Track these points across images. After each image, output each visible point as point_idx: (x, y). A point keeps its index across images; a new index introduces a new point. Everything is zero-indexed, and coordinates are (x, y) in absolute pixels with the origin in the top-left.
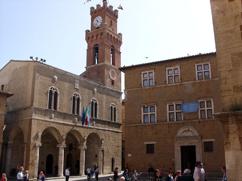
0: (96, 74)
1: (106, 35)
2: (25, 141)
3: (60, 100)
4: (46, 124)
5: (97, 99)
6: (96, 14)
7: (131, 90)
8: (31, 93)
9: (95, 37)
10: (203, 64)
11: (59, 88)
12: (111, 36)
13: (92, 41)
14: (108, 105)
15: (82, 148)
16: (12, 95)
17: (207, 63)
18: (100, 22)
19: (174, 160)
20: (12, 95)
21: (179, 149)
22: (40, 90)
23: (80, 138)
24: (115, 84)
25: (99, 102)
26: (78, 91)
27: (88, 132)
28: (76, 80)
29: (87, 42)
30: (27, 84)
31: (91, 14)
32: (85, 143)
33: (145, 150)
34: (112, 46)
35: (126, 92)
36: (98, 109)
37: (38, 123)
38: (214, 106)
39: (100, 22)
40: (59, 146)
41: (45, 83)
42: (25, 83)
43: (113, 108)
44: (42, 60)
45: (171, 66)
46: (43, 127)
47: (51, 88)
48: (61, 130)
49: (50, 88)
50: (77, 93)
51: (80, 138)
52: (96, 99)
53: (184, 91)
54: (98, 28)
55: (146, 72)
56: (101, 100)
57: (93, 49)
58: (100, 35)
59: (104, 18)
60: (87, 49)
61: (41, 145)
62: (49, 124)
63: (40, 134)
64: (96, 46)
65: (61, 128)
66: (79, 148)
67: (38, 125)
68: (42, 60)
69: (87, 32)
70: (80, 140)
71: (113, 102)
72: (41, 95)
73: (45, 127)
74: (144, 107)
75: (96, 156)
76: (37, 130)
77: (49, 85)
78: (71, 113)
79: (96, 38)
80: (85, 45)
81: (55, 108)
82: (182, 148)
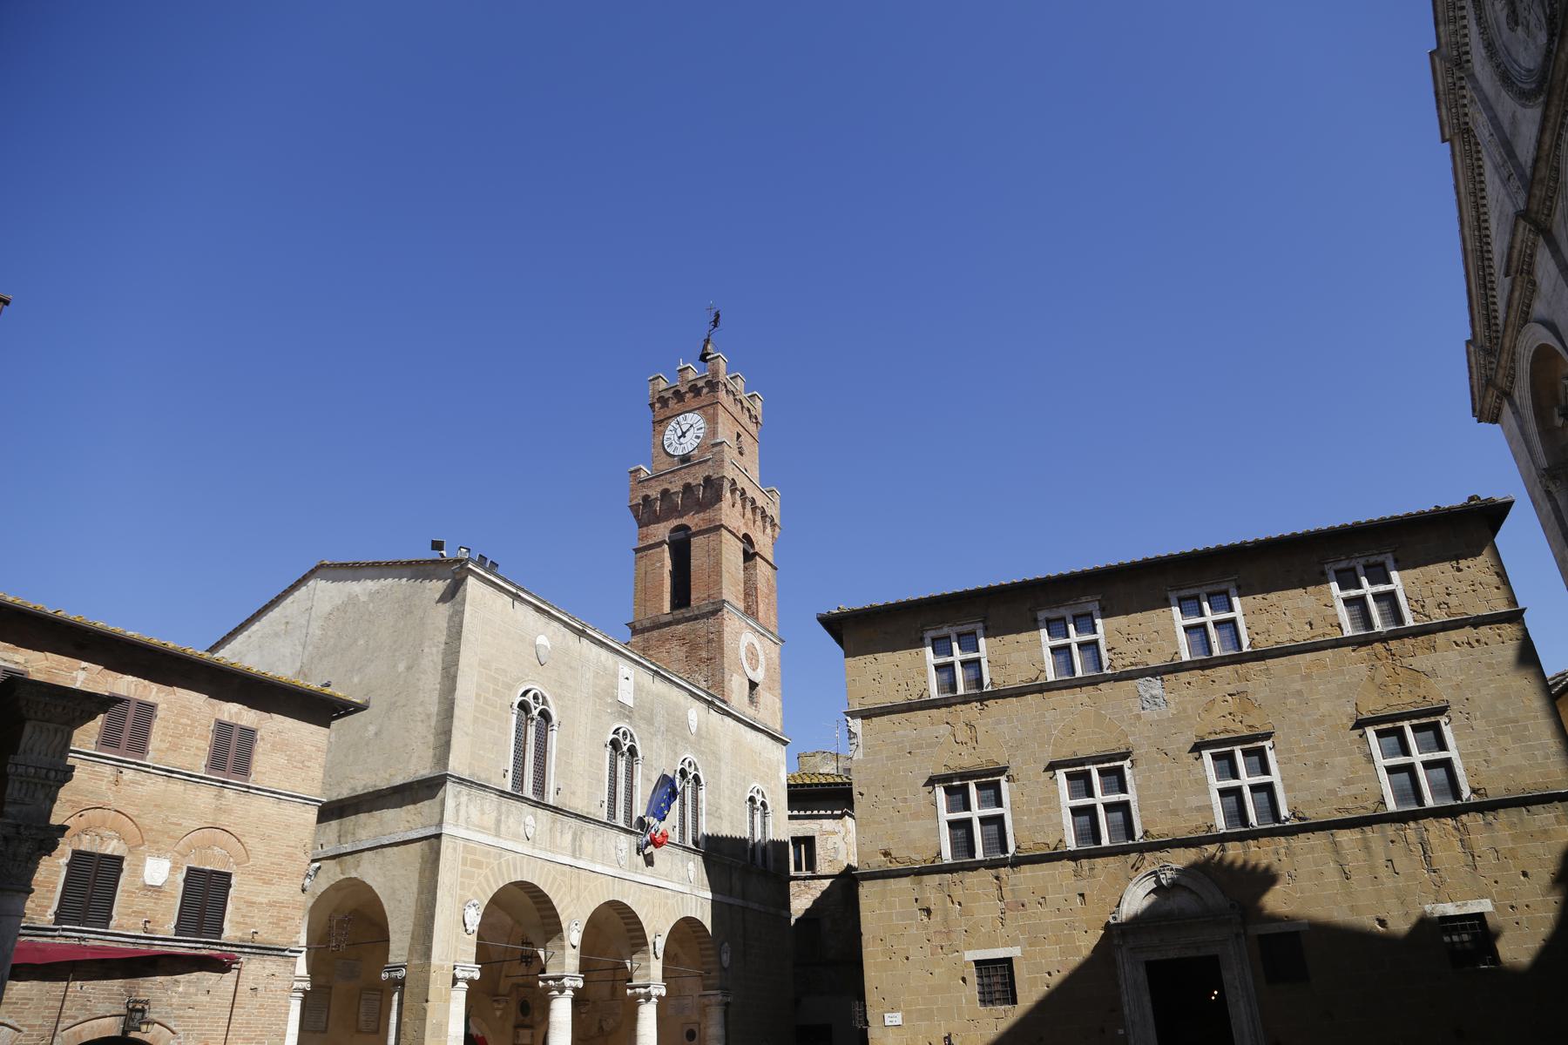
0: (682, 655)
2: (399, 949)
3: (560, 751)
10: (1202, 592)
11: (558, 697)
12: (743, 492)
14: (739, 791)
16: (359, 708)
17: (1223, 587)
19: (1121, 1032)
20: (359, 708)
21: (1142, 975)
22: (478, 696)
26: (629, 717)
30: (409, 668)
32: (656, 968)
33: (973, 989)
34: (746, 536)
36: (703, 806)
37: (464, 863)
38: (1281, 770)
42: (401, 667)
44: (483, 559)
45: (1059, 603)
47: (525, 693)
48: (561, 900)
50: (625, 726)
53: (1130, 711)
54: (685, 459)
55: (945, 630)
59: (712, 421)
61: (477, 976)
63: (474, 918)
64: (681, 535)
68: (483, 559)
73: (496, 882)
74: (948, 791)
75: (691, 1035)
78: (603, 815)
81: (540, 786)
82: (1152, 968)
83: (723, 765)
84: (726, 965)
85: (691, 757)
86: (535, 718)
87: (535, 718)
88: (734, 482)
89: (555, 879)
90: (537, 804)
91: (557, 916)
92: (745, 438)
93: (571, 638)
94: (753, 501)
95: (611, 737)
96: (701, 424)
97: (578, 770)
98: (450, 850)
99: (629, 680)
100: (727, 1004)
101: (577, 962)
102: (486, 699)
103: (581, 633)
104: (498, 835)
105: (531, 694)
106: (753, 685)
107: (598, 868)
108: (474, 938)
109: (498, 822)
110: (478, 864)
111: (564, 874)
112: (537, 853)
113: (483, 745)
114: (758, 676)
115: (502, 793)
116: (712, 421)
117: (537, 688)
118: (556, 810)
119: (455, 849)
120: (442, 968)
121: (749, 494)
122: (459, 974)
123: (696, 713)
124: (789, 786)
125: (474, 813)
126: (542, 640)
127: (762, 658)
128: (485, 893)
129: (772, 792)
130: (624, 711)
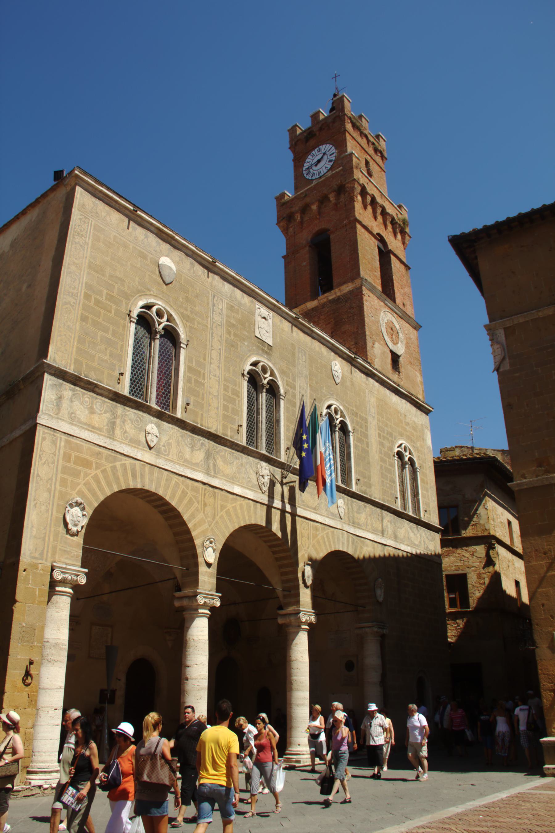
1: (358, 189)
3: (189, 369)
4: (114, 468)
5: (344, 406)
6: (312, 142)
7: (521, 320)
8: (43, 308)
9: (314, 207)
11: (184, 317)
12: (373, 199)
13: (302, 222)
14: (387, 444)
15: (292, 618)
18: (330, 161)
22: (87, 297)
23: (282, 574)
24: (402, 370)
25: (352, 422)
27: (318, 542)
28: (257, 306)
29: (285, 231)
31: (293, 147)
32: (306, 596)
35: (501, 334)
37: (67, 458)
39: (330, 161)
40: (185, 602)
41: (118, 274)
43: (406, 459)
46: (98, 482)
47: (148, 307)
48: (193, 516)
49: (141, 303)
50: (264, 361)
51: (282, 574)
52: (342, 408)
56: (361, 417)
57: (307, 248)
58: (332, 197)
60: (284, 253)
61: (83, 580)
62: (134, 476)
63: (79, 518)
65: (196, 504)
66: (280, 621)
67: (71, 465)
69: (281, 203)
70: (283, 582)
71: (401, 435)
72: (95, 324)
73: (109, 485)
75: (350, 666)
76: (62, 495)
77: (139, 291)
78: (243, 440)
79: (319, 208)
80: (278, 243)
83: (370, 419)
84: (381, 599)
85: (336, 404)
86: (158, 334)
87: (158, 334)
88: (363, 189)
89: (184, 493)
90: (160, 416)
91: (188, 532)
92: (371, 163)
93: (200, 270)
94: (383, 208)
95: (248, 368)
96: (333, 150)
97: (211, 386)
98: (47, 443)
99: (268, 324)
100: (383, 636)
101: (214, 581)
102: (97, 302)
103: (210, 268)
104: (111, 436)
105: (154, 309)
106: (395, 358)
107: (237, 490)
108: (79, 540)
109: (112, 425)
110: (87, 464)
111: (196, 490)
112: (161, 463)
113: (84, 331)
114: (400, 349)
115: (117, 398)
116: (341, 145)
117: (160, 304)
118: (181, 424)
119: (54, 442)
120: (35, 566)
121: (379, 200)
122: (58, 576)
123: (338, 366)
124: (435, 462)
125: (82, 413)
126: (165, 261)
127: (401, 335)
128: (94, 494)
129: (418, 451)
130: (265, 348)
